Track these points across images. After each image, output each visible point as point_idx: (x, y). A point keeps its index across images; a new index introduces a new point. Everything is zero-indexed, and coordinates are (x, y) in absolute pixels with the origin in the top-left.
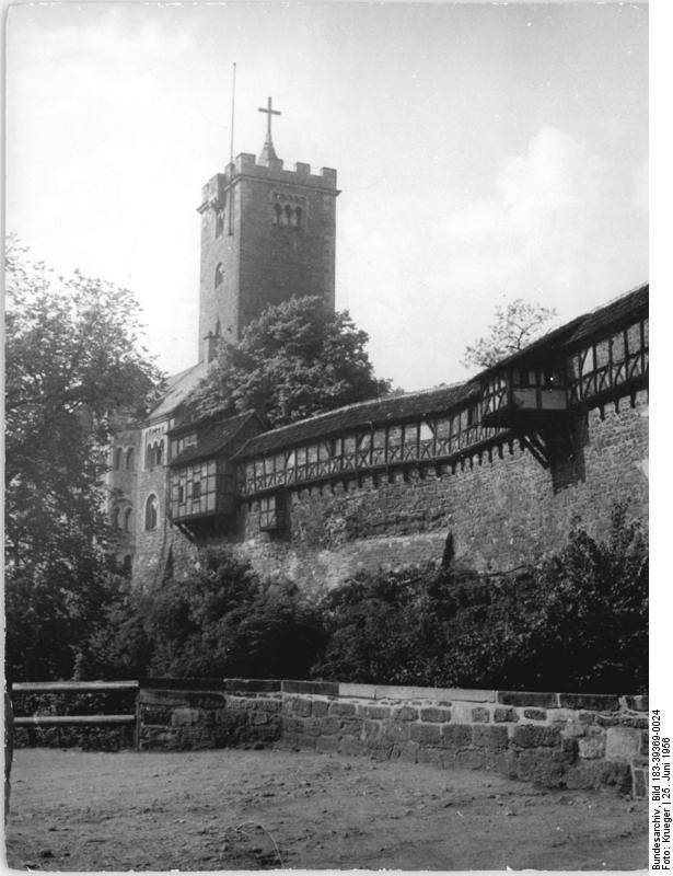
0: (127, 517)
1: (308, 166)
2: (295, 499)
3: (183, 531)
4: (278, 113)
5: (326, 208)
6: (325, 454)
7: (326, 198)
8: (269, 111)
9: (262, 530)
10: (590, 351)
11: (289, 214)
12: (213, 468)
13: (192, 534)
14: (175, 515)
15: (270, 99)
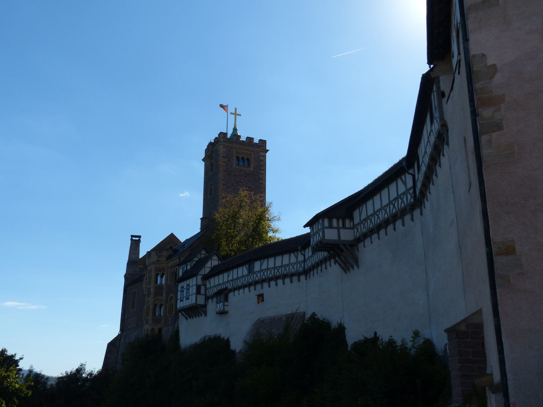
0: (161, 308)
1: (253, 139)
2: (231, 295)
3: (183, 315)
4: (240, 115)
5: (261, 158)
6: (246, 272)
7: (262, 154)
8: (236, 114)
9: (217, 313)
10: (364, 205)
11: (244, 162)
12: (195, 283)
13: (187, 316)
14: (178, 307)
15: (236, 109)
